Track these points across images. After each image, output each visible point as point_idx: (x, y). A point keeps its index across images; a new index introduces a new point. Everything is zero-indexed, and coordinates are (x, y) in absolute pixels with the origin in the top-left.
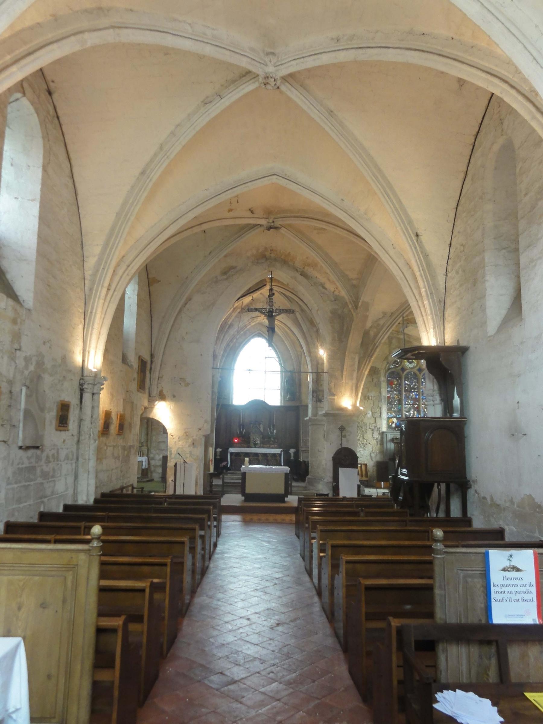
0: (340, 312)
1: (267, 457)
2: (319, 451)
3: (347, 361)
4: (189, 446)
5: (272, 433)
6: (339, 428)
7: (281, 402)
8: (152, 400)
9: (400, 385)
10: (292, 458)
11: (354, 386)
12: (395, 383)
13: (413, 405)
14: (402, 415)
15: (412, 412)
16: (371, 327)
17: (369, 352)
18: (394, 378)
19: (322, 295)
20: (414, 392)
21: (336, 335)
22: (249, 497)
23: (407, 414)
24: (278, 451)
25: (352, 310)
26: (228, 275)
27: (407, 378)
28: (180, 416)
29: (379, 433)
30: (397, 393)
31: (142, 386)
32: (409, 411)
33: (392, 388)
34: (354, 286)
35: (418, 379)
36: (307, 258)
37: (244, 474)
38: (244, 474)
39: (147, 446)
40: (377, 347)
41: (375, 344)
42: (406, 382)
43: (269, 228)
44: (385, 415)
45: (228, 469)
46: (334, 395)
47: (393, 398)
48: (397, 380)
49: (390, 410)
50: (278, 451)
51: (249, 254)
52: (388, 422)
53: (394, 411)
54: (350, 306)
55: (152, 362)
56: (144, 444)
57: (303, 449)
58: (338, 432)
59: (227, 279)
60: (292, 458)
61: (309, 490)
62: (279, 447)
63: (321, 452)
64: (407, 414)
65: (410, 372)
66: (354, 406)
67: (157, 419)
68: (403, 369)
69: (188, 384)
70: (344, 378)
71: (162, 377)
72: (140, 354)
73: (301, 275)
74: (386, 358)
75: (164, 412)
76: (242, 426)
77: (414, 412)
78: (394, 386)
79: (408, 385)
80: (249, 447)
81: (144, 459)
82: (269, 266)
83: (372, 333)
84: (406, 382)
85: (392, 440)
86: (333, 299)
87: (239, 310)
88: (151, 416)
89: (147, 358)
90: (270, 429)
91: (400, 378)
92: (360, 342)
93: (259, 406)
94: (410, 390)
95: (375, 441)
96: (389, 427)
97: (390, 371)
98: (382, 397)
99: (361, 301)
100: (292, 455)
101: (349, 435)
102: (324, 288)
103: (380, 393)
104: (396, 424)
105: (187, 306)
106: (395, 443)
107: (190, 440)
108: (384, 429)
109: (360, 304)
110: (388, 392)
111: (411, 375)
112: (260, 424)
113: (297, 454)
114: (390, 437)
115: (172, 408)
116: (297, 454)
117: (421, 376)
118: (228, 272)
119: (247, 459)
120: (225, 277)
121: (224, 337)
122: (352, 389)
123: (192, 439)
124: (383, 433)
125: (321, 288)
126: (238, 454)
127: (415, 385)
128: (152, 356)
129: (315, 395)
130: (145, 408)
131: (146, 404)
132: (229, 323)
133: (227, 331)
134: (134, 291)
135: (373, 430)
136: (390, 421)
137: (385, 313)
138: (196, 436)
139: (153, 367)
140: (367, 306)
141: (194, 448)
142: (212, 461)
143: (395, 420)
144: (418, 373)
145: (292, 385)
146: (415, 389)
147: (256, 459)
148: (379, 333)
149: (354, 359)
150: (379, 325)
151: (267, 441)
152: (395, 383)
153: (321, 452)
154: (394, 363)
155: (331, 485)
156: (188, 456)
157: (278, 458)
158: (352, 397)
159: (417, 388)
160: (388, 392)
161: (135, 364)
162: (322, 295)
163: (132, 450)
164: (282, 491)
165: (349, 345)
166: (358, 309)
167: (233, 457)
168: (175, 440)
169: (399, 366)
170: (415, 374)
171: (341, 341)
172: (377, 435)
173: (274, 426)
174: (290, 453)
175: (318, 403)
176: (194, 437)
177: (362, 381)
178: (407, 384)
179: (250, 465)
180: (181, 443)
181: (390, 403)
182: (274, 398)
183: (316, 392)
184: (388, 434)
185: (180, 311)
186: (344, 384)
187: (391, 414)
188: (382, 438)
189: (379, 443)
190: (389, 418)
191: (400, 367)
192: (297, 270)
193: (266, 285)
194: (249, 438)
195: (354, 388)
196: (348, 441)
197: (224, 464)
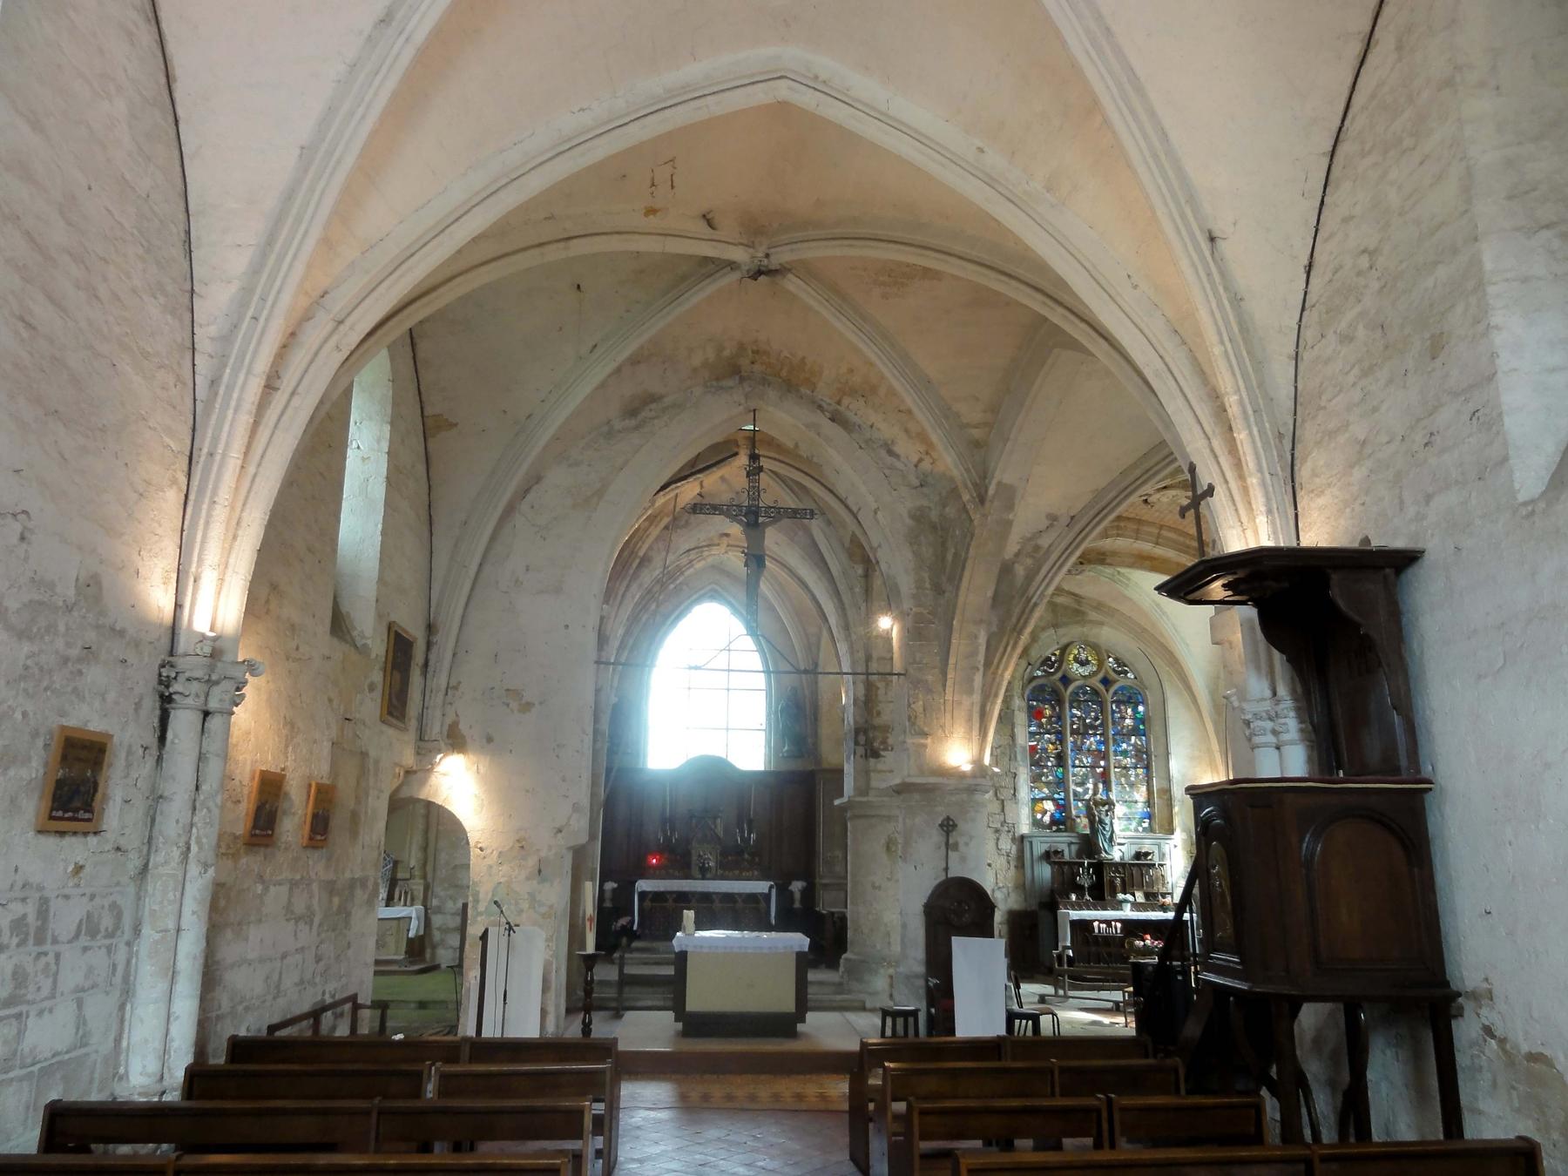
0: (934, 515)
1: (735, 902)
2: (874, 887)
3: (958, 644)
4: (528, 879)
5: (746, 841)
6: (941, 826)
7: (768, 762)
8: (426, 749)
9: (1060, 718)
10: (797, 905)
11: (976, 709)
12: (1048, 712)
13: (1093, 767)
14: (1066, 791)
15: (1090, 786)
16: (1017, 555)
17: (1014, 620)
18: (1044, 701)
19: (887, 472)
21: (926, 575)
22: (696, 1025)
23: (1080, 790)
24: (761, 887)
25: (970, 507)
26: (640, 417)
27: (1075, 701)
28: (505, 795)
29: (1013, 839)
30: (1053, 737)
31: (395, 707)
32: (1082, 784)
33: (1040, 726)
34: (977, 444)
35: (1101, 704)
36: (851, 371)
37: (681, 958)
38: (681, 958)
39: (424, 877)
40: (1036, 605)
41: (1029, 600)
43: (757, 273)
44: (1024, 793)
45: (633, 936)
46: (925, 735)
48: (1053, 708)
49: (1036, 779)
50: (761, 887)
51: (697, 360)
52: (1033, 811)
53: (1048, 784)
54: (966, 497)
55: (429, 645)
56: (417, 873)
57: (825, 881)
58: (936, 836)
59: (637, 428)
60: (797, 905)
61: (849, 992)
62: (764, 877)
63: (879, 888)
64: (1080, 790)
65: (1081, 687)
66: (978, 762)
67: (439, 802)
68: (1066, 680)
69: (527, 707)
70: (949, 690)
71: (456, 688)
72: (393, 618)
73: (833, 420)
75: (459, 785)
76: (668, 822)
77: (1095, 785)
80: (687, 877)
81: (414, 912)
82: (747, 397)
83: (1020, 570)
85: (1047, 856)
86: (916, 482)
87: (666, 520)
88: (423, 795)
89: (416, 632)
90: (742, 832)
91: (1060, 702)
92: (990, 594)
93: (715, 774)
94: (1083, 732)
95: (1003, 860)
96: (1037, 823)
97: (1034, 684)
98: (1018, 750)
99: (994, 482)
100: (797, 896)
101: (967, 844)
102: (891, 453)
103: (1013, 737)
105: (529, 497)
106: (1052, 864)
107: (532, 862)
108: (1025, 828)
109: (991, 491)
110: (1032, 734)
111: (1085, 693)
112: (715, 818)
113: (809, 894)
114: (1040, 848)
115: (482, 770)
116: (809, 894)
117: (1109, 697)
118: (639, 409)
119: (689, 915)
120: (633, 422)
121: (628, 587)
122: (970, 720)
123: (536, 859)
124: (1022, 837)
125: (883, 453)
126: (658, 896)
127: (1096, 719)
128: (430, 628)
129: (862, 739)
130: (408, 772)
131: (409, 759)
132: (641, 554)
133: (635, 576)
134: (378, 441)
135: (997, 831)
137: (1053, 518)
138: (550, 848)
139: (432, 657)
140: (1009, 496)
141: (543, 881)
142: (591, 920)
143: (1049, 805)
144: (1101, 687)
145: (798, 717)
146: (1095, 728)
147: (714, 911)
148: (1039, 568)
149: (976, 637)
150: (1037, 548)
151: (734, 861)
152: (1048, 712)
153: (879, 888)
154: (1043, 664)
155: (921, 982)
156: (525, 905)
157: (763, 905)
158: (970, 740)
161: (379, 647)
162: (887, 472)
163: (359, 892)
164: (789, 1005)
165: (961, 599)
166: (987, 504)
167: (647, 904)
168: (488, 861)
169: (1057, 670)
170: (1095, 692)
171: (938, 590)
172: (1006, 844)
173: (750, 822)
174: (792, 893)
175: (872, 761)
176: (543, 854)
177: (996, 696)
178: (1074, 716)
179: (698, 929)
180: (505, 868)
181: (1035, 763)
182: (751, 752)
183: (865, 732)
184: (1035, 841)
185: (510, 510)
186: (949, 708)
188: (1021, 852)
189: (1013, 864)
190: (1035, 801)
191: (1059, 675)
192: (820, 407)
193: (736, 454)
194: (688, 854)
195: (976, 717)
196: (963, 859)
197: (623, 921)
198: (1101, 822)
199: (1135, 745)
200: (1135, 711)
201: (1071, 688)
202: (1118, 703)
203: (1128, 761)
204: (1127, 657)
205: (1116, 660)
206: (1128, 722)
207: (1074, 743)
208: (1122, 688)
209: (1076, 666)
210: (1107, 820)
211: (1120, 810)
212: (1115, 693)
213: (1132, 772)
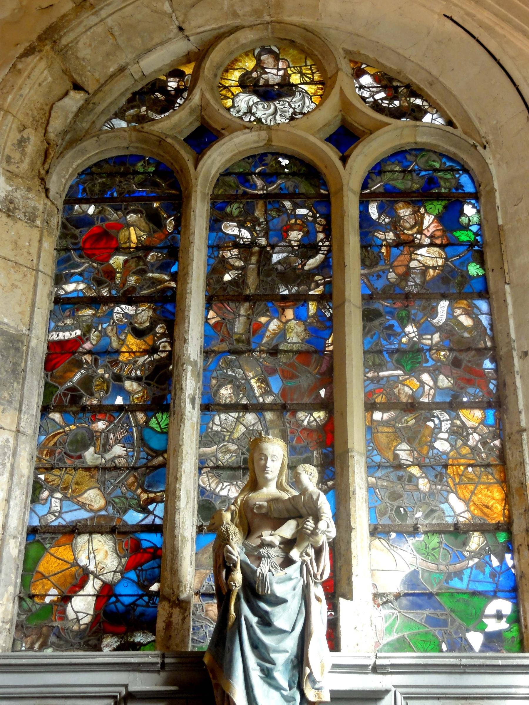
9: (174, 252)
13: (283, 408)
18: (123, 203)
20: (299, 300)
30: (144, 314)
35: (325, 203)
42: (231, 229)
47: (106, 354)
48: (155, 220)
52: (29, 570)
74: (50, 35)
78: (117, 261)
79: (245, 249)
84: (231, 229)
104: (106, 593)
117: (352, 173)
127: (309, 248)
136: (48, 565)
143: (101, 555)
154: (137, 98)
159: (325, 265)
160: (62, 304)
187: (70, 494)
190: (38, 536)
198: (254, 591)
199: (449, 330)
200: (450, 219)
201: (218, 158)
202: (390, 198)
203: (429, 385)
204: (414, 62)
205: (385, 81)
206: (428, 257)
207: (212, 332)
208: (399, 154)
209: (245, 100)
210: (285, 583)
211: (382, 565)
212: (377, 169)
213: (444, 421)
